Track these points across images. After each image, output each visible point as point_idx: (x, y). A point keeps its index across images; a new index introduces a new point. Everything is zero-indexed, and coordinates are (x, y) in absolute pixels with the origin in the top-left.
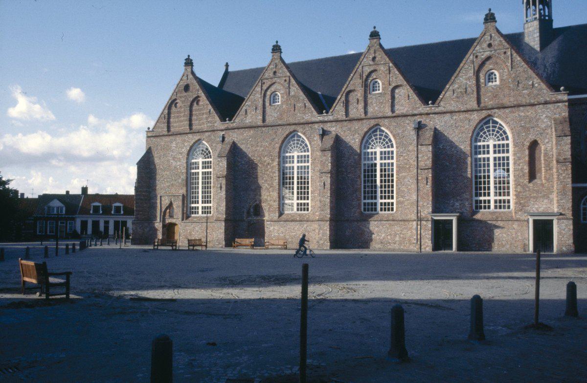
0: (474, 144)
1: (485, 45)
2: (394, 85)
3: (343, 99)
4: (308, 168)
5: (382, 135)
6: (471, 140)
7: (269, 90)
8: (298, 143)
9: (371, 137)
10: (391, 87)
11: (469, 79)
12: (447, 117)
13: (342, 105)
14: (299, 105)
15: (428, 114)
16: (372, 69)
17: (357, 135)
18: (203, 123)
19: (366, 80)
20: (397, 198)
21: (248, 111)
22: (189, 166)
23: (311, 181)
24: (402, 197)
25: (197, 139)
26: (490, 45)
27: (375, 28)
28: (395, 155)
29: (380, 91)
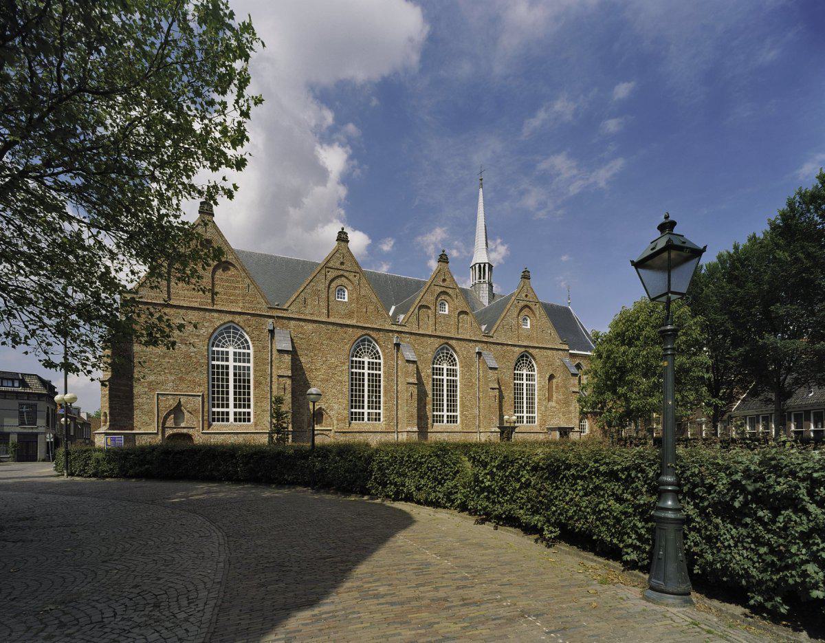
0: (351, 359)
1: (524, 295)
2: (460, 310)
3: (417, 310)
4: (380, 377)
5: (448, 354)
6: (208, 345)
7: (335, 282)
8: (234, 337)
9: (439, 354)
10: (458, 311)
11: (513, 319)
12: (499, 347)
13: (415, 317)
14: (371, 308)
15: (486, 343)
16: (440, 291)
17: (429, 349)
18: (236, 302)
19: (437, 299)
20: (462, 412)
21: (309, 301)
22: (211, 356)
23: (385, 390)
24: (466, 411)
25: (226, 320)
26: (526, 296)
27: (444, 251)
28: (252, 358)
29: (447, 312)
